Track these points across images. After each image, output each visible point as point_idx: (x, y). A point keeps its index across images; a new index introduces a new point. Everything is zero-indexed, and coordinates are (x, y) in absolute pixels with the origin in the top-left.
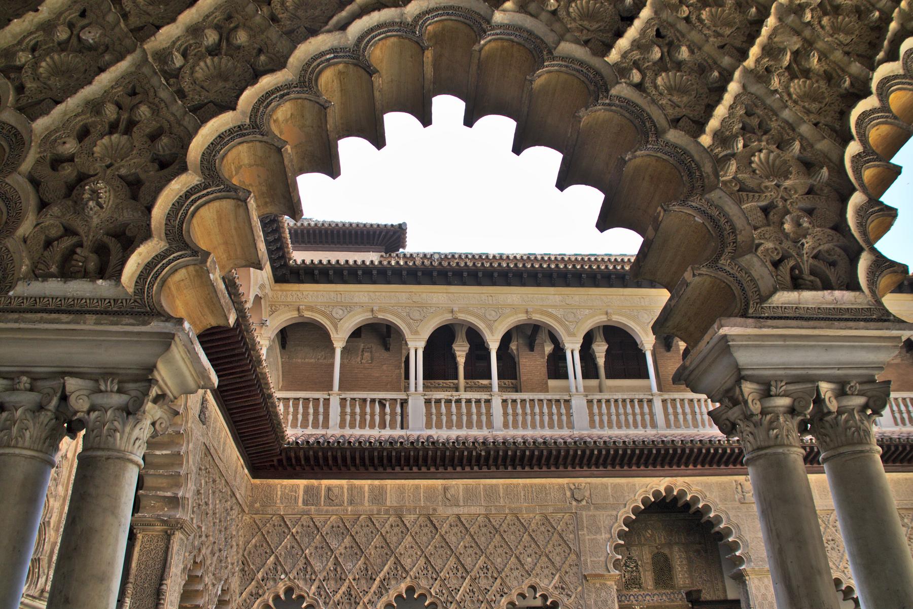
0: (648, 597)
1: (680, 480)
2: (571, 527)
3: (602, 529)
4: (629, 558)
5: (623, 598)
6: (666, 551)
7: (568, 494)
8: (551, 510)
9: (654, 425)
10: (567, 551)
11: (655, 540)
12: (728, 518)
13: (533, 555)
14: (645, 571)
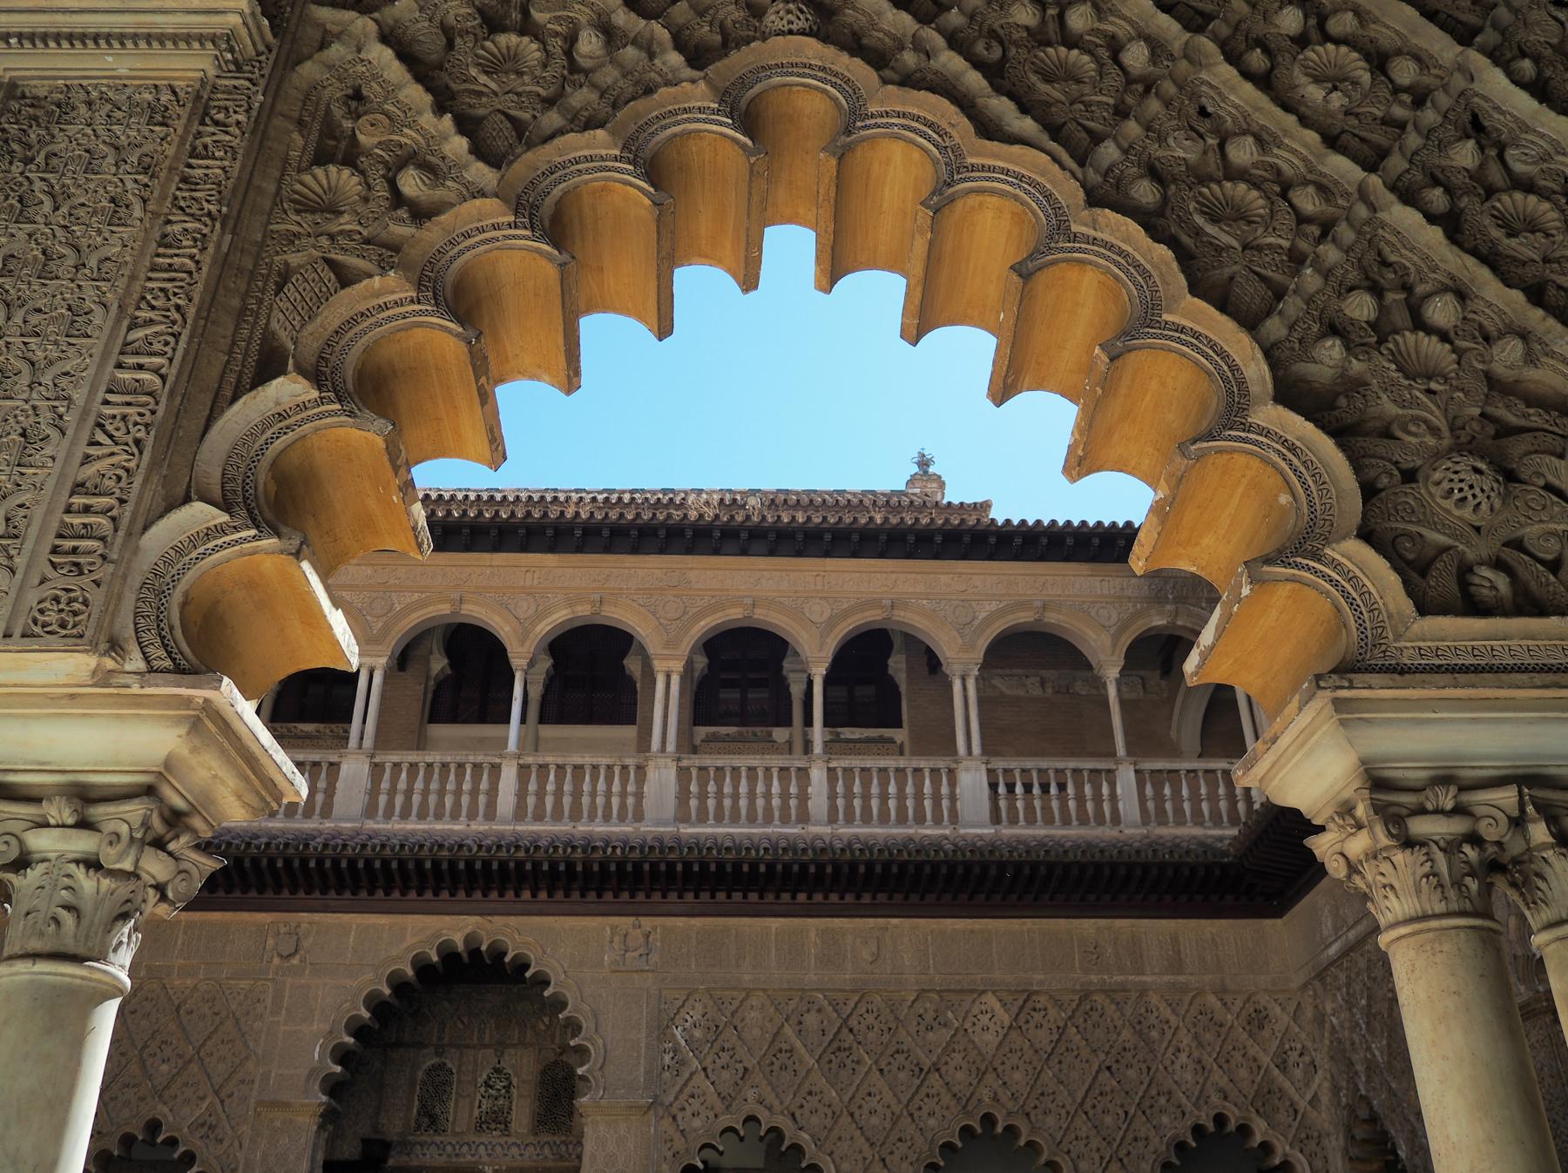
0: (514, 1150)
1: (498, 920)
4: (497, 1071)
5: (465, 1148)
9: (491, 814)
14: (521, 1096)
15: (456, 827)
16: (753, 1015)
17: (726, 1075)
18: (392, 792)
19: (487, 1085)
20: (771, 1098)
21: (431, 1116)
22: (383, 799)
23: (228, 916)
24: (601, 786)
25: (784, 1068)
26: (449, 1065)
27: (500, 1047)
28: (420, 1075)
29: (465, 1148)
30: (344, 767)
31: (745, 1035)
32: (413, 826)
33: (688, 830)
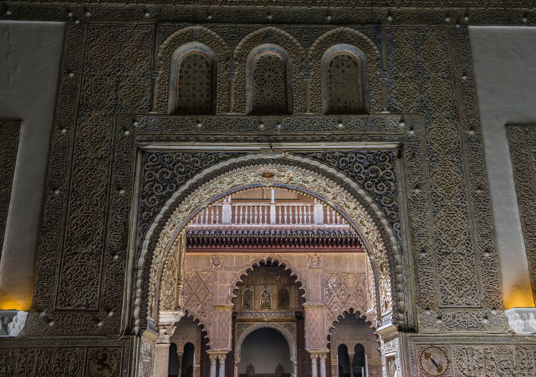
0: (273, 314)
2: (211, 279)
3: (228, 281)
4: (265, 292)
5: (259, 314)
6: (287, 288)
7: (211, 261)
8: (200, 270)
9: (269, 222)
10: (207, 292)
11: (281, 282)
12: (301, 276)
13: (189, 294)
14: (273, 299)
15: (259, 226)
16: (350, 281)
17: (343, 297)
18: (239, 215)
19: (263, 295)
20: (356, 303)
21: (247, 305)
22: (236, 217)
23: (198, 254)
24: (301, 213)
25: (360, 295)
26: (251, 290)
27: (266, 285)
28: (243, 293)
29: (259, 314)
30: (223, 207)
31: (348, 286)
32: (246, 225)
33: (327, 226)
